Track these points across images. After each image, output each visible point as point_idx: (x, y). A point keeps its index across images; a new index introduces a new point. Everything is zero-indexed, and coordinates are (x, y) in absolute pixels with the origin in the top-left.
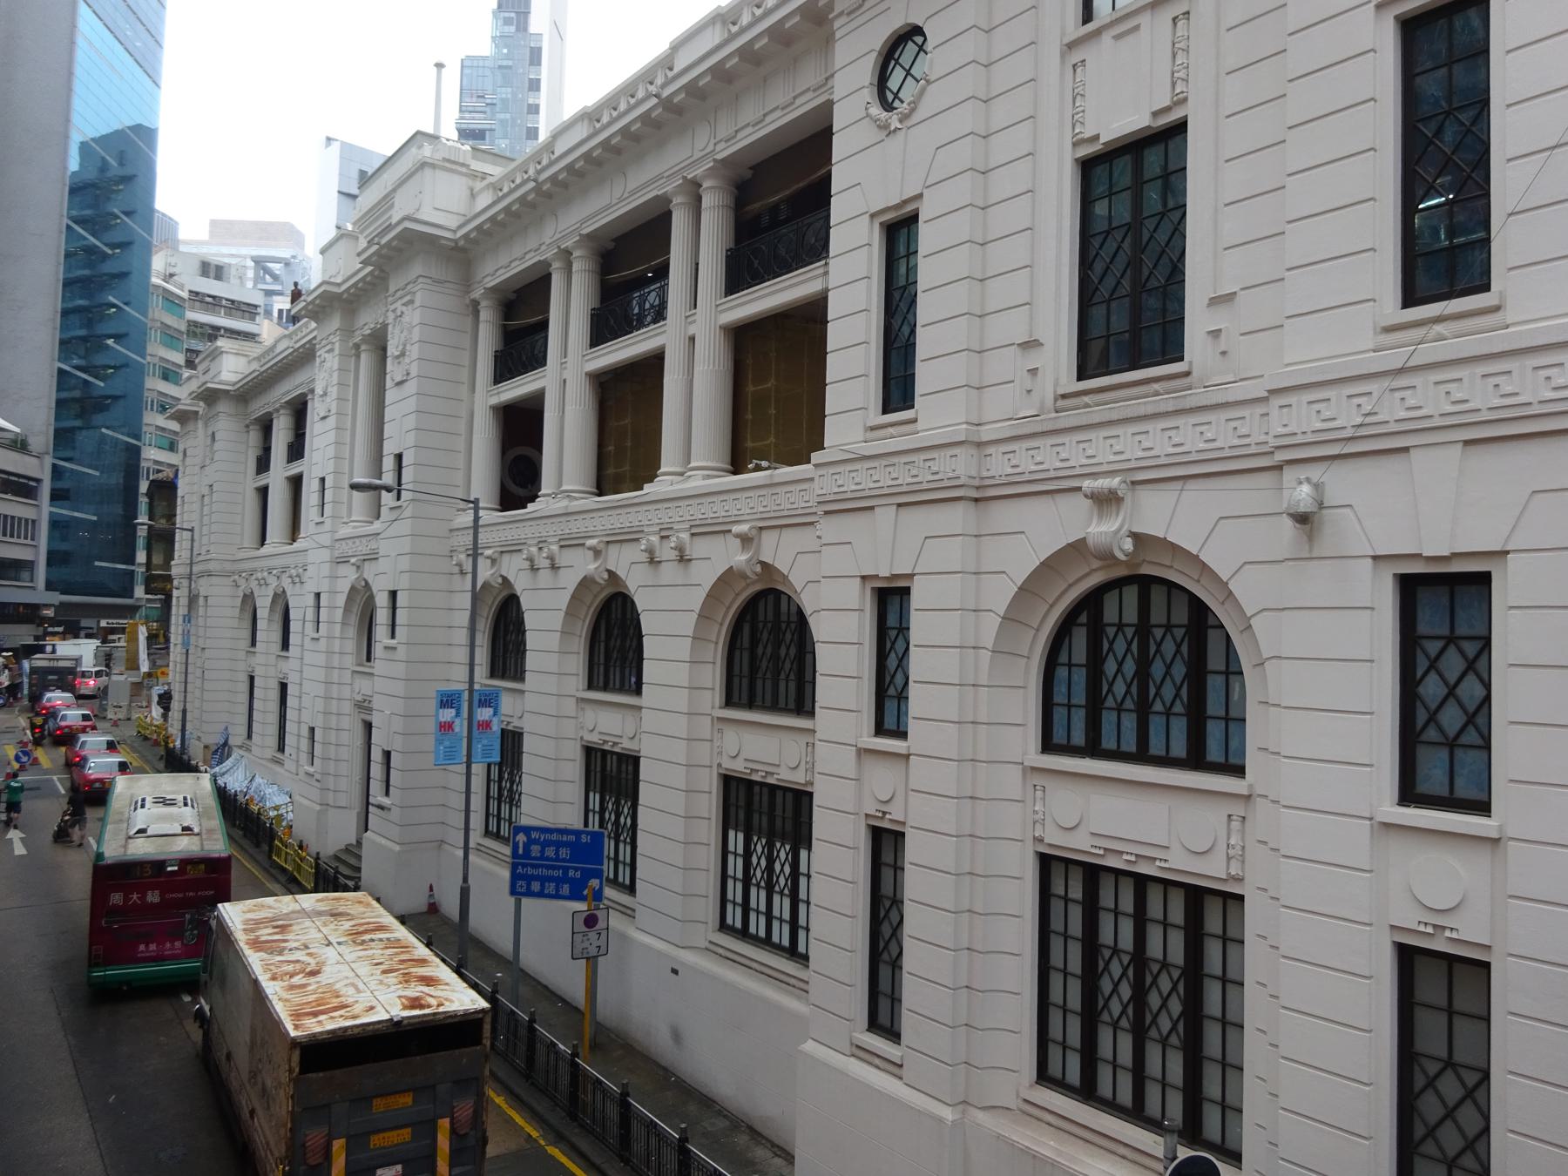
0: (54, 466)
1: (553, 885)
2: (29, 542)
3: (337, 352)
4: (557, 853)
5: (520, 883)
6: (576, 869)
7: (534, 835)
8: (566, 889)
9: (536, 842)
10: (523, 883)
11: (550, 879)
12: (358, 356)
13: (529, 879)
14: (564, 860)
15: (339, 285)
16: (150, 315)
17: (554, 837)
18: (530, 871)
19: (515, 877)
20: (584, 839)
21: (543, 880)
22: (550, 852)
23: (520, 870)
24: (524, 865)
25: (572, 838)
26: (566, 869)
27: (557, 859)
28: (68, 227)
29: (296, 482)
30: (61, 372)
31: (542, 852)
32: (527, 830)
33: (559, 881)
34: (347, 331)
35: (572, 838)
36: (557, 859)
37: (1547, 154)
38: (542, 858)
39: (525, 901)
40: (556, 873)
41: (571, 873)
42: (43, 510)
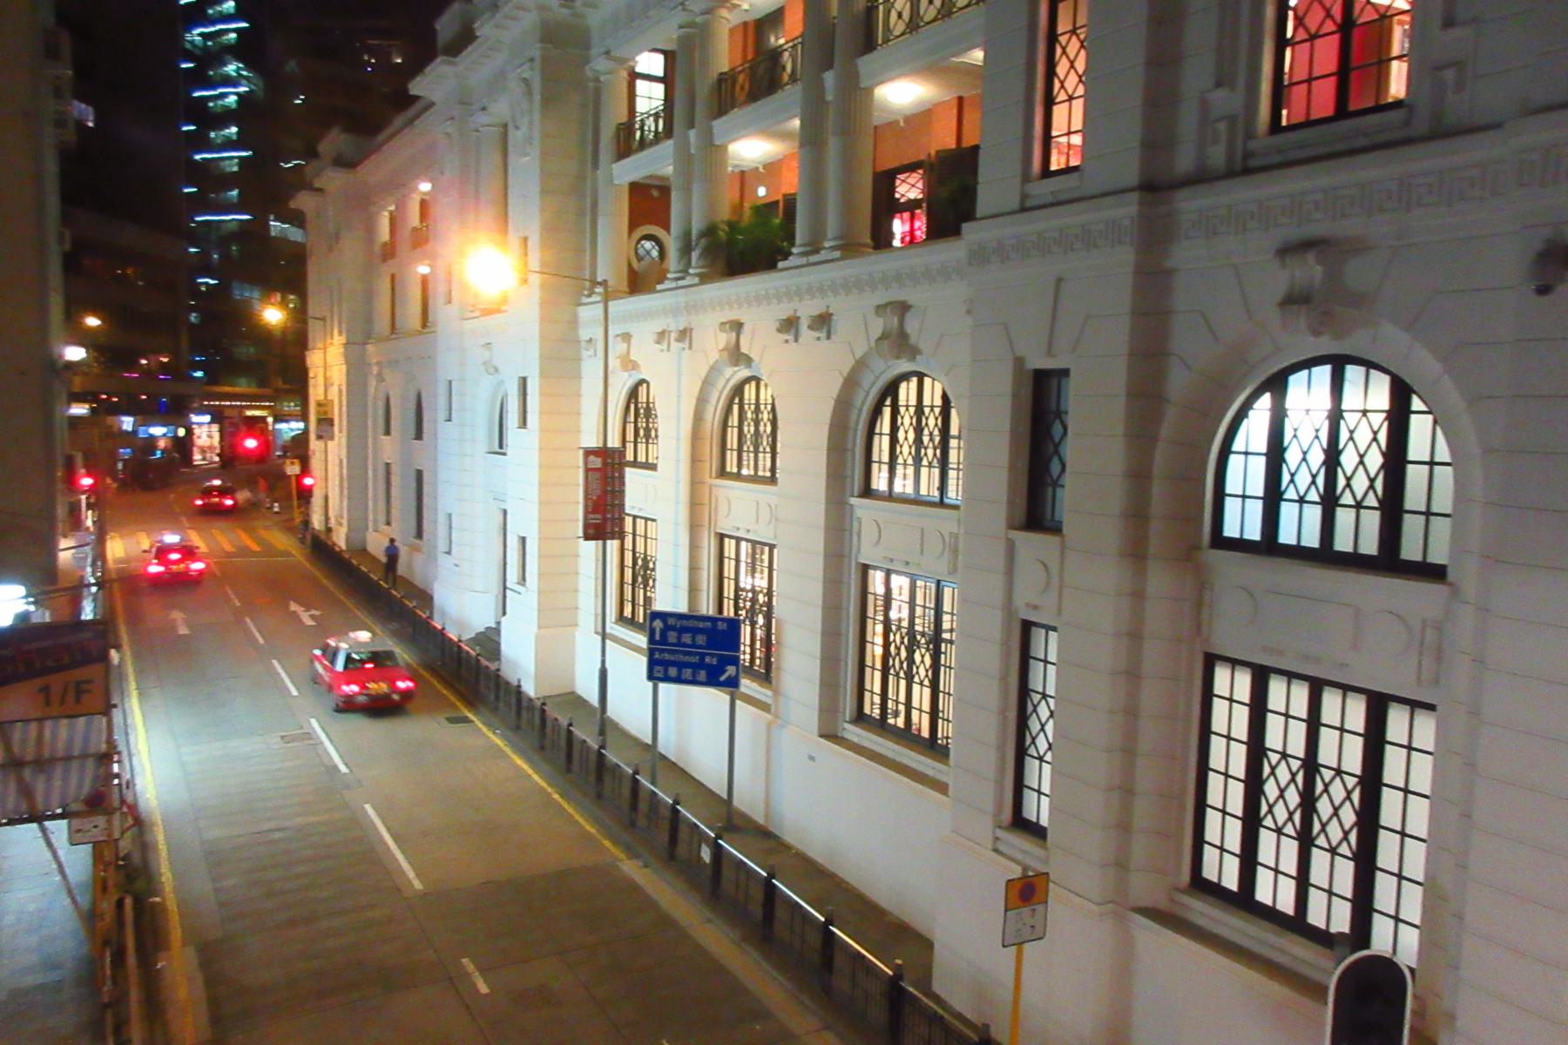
1: (689, 671)
5: (658, 668)
7: (671, 621)
8: (702, 675)
9: (673, 628)
10: (660, 668)
13: (666, 664)
18: (667, 656)
19: (652, 663)
20: (721, 626)
21: (680, 666)
22: (687, 638)
26: (702, 656)
35: (709, 624)
36: (694, 646)
39: (662, 686)
40: (695, 659)
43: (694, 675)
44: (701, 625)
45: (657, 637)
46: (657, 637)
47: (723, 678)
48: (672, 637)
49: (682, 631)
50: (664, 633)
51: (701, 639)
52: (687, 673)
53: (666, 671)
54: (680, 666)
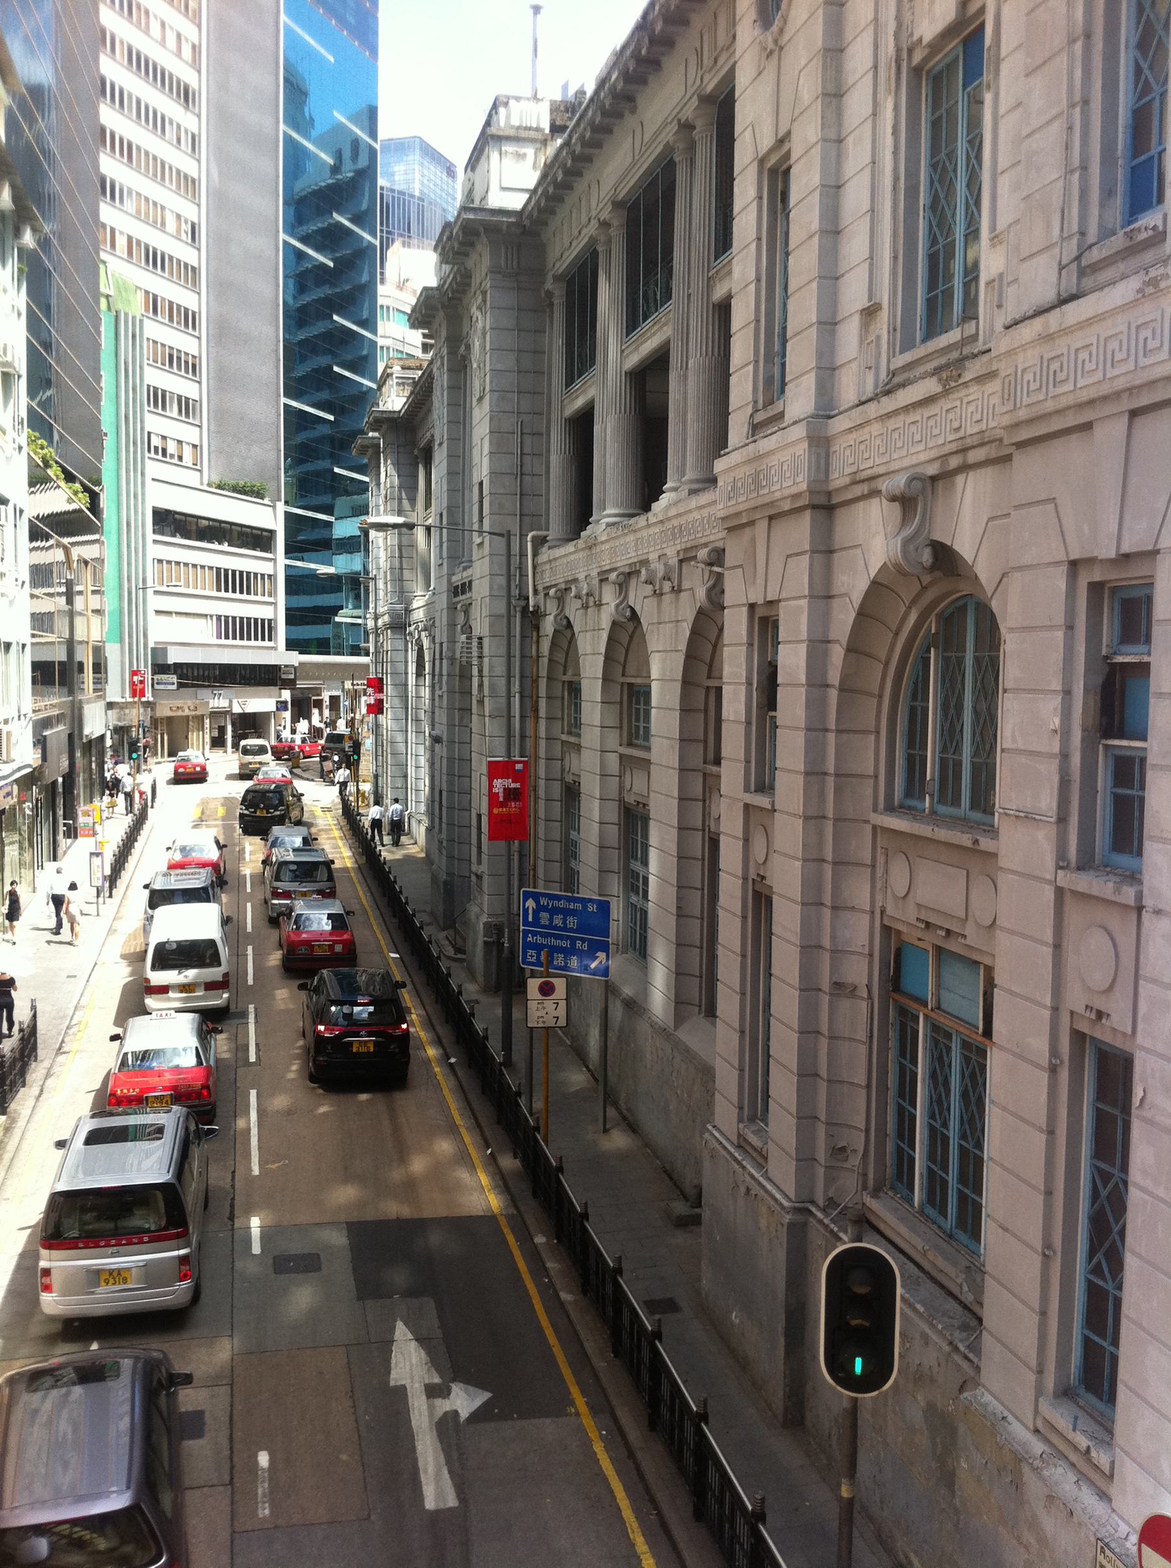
2: (267, 599)
4: (564, 922)
5: (530, 952)
6: (583, 940)
9: (545, 909)
10: (533, 952)
14: (571, 930)
16: (380, 331)
21: (553, 950)
22: (558, 920)
24: (534, 934)
26: (573, 940)
31: (551, 920)
35: (579, 906)
36: (565, 929)
37: (796, 115)
40: (566, 944)
42: (275, 564)
45: (530, 919)
46: (530, 919)
48: (544, 916)
49: (554, 911)
51: (572, 922)
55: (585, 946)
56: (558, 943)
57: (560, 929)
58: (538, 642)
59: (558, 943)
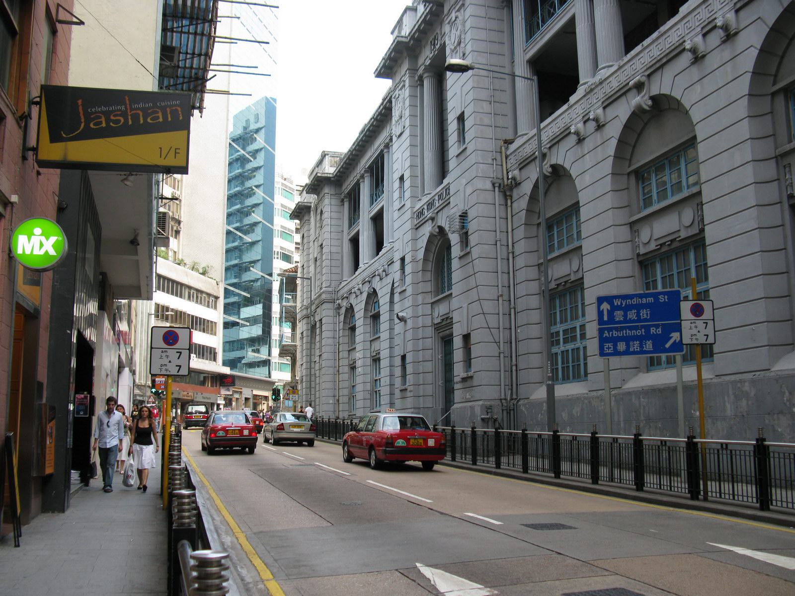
0: (225, 289)
3: (407, 84)
4: (638, 315)
6: (657, 326)
7: (617, 302)
8: (649, 345)
9: (619, 308)
11: (634, 338)
12: (422, 85)
13: (615, 341)
14: (645, 320)
15: (406, 37)
17: (635, 301)
18: (615, 334)
21: (627, 340)
22: (632, 315)
23: (606, 334)
24: (609, 330)
25: (651, 300)
27: (639, 320)
28: (230, 144)
29: (378, 219)
30: (229, 233)
32: (609, 299)
33: (641, 339)
34: (413, 70)
35: (651, 300)
36: (639, 320)
38: (626, 321)
41: (653, 330)
43: (641, 346)
44: (644, 301)
45: (606, 318)
46: (606, 318)
47: (667, 346)
48: (619, 315)
50: (611, 313)
51: (645, 314)
52: (635, 346)
53: (615, 346)
54: (627, 340)
55: (659, 331)
56: (634, 332)
57: (634, 321)
58: (511, 206)
59: (634, 332)
